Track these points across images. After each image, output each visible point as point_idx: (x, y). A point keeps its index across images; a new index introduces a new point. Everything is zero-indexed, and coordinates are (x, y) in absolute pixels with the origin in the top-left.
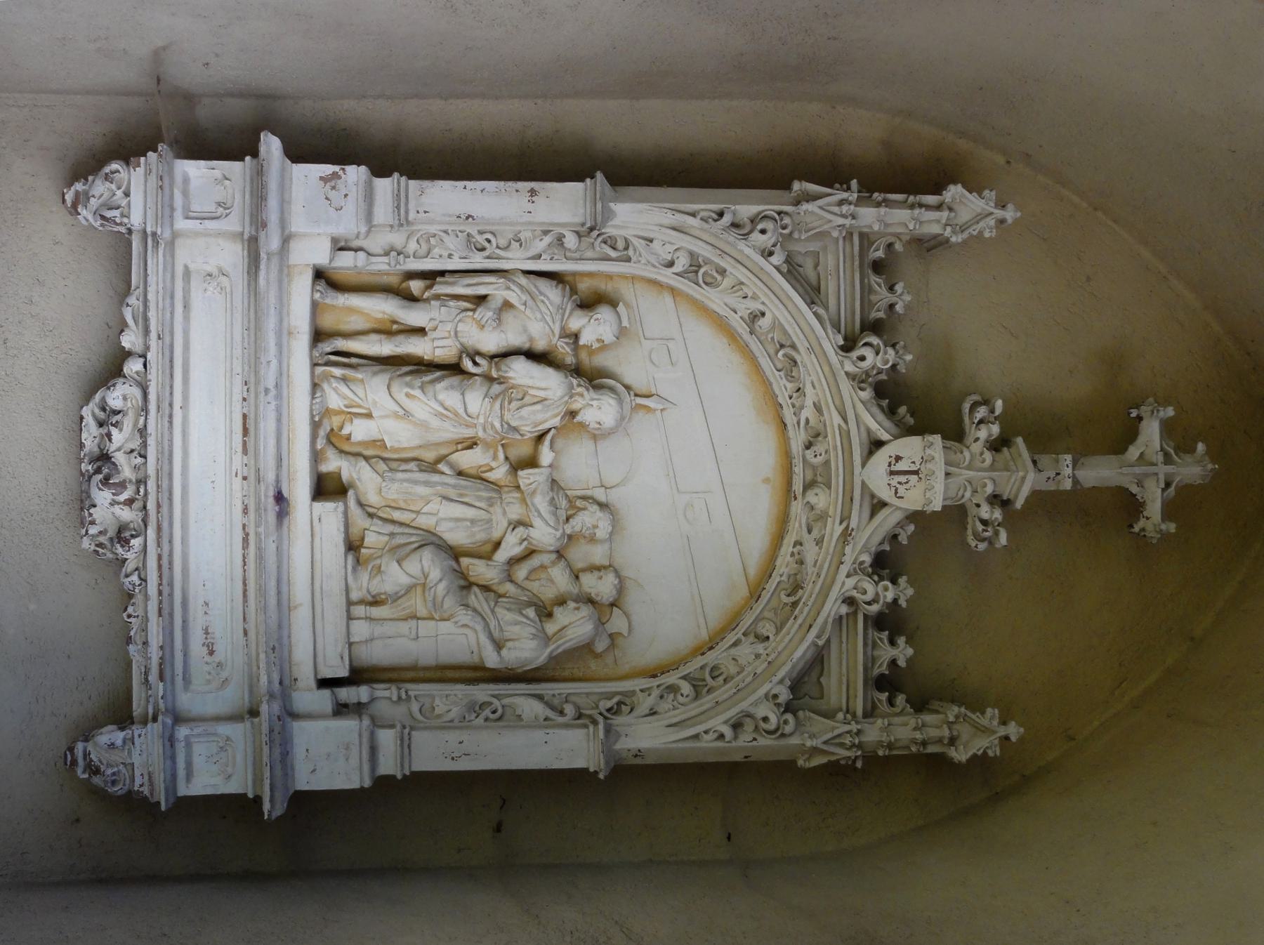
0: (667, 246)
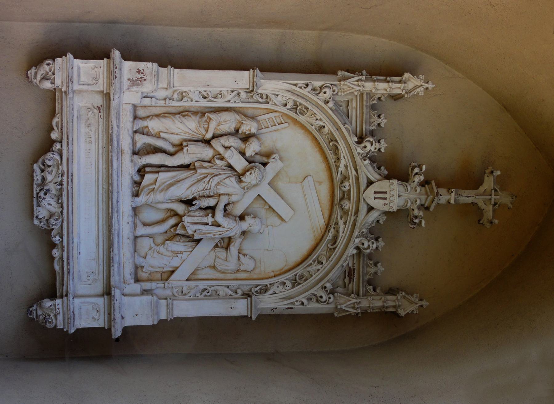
0: (284, 98)
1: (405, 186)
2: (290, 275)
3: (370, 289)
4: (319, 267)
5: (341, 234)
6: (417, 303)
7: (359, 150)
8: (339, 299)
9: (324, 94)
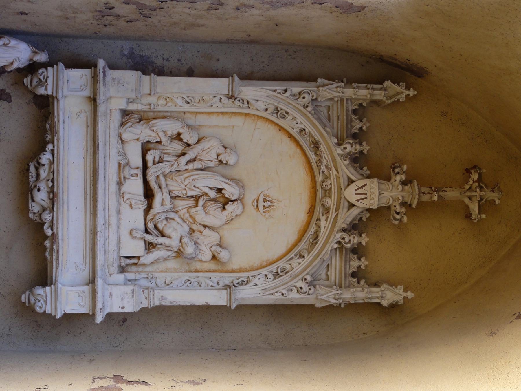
1: (387, 185)
2: (273, 268)
3: (354, 282)
4: (300, 260)
5: (322, 230)
6: (403, 294)
7: (339, 151)
8: (320, 290)
9: (303, 100)
